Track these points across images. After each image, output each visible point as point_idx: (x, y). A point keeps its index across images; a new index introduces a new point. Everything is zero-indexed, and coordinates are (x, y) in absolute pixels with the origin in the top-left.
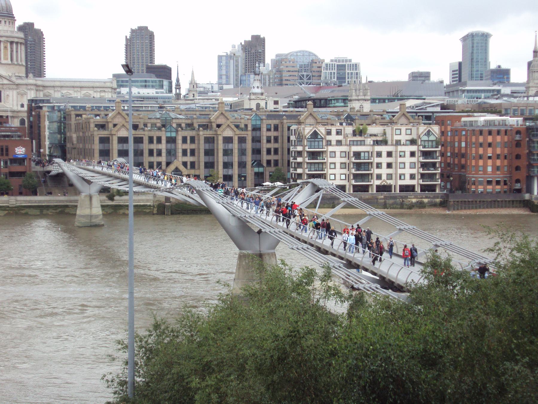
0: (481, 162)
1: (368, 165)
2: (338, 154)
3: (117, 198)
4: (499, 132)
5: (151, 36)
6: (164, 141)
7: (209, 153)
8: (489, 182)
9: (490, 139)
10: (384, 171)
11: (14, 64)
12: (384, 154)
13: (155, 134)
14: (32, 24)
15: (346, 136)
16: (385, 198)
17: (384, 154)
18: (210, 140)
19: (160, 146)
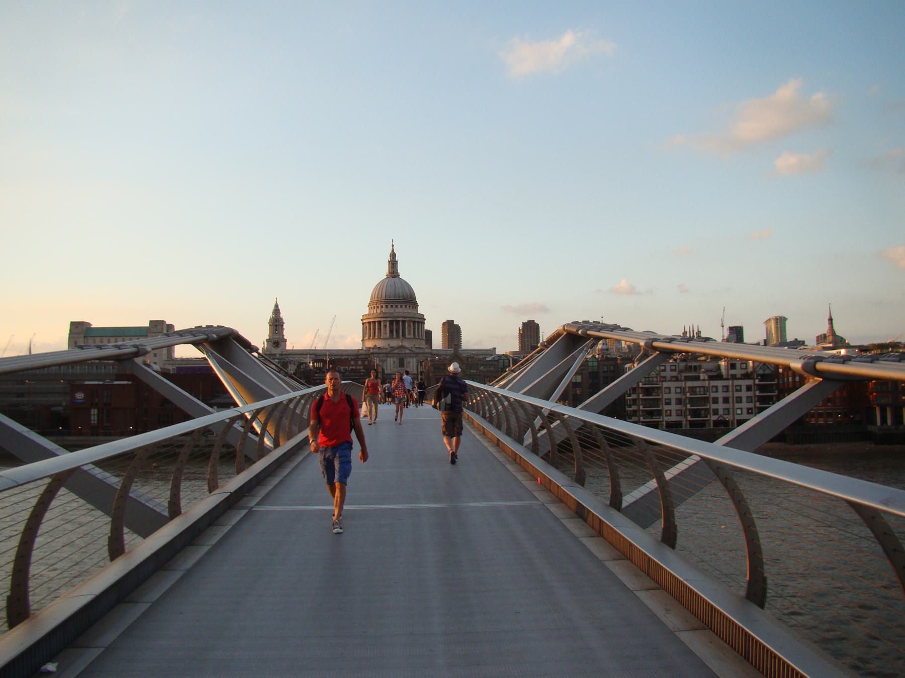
1: (705, 400)
2: (673, 390)
5: (537, 326)
10: (720, 406)
17: (720, 389)
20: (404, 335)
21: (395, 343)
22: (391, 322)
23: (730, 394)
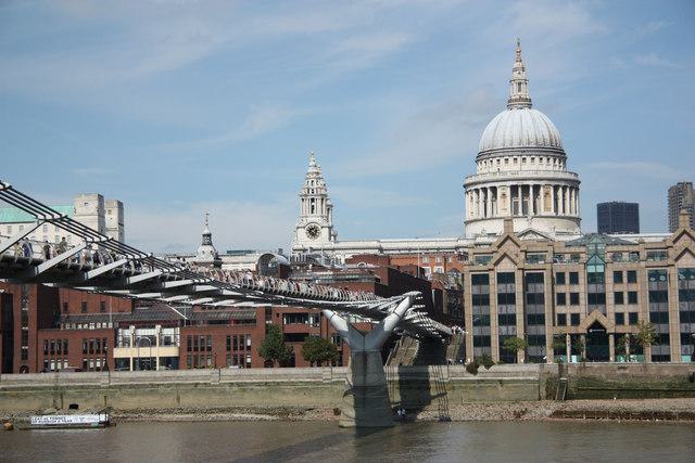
3: (482, 368)
6: (582, 279)
7: (658, 296)
11: (559, 217)
13: (566, 267)
19: (575, 289)
22: (514, 189)
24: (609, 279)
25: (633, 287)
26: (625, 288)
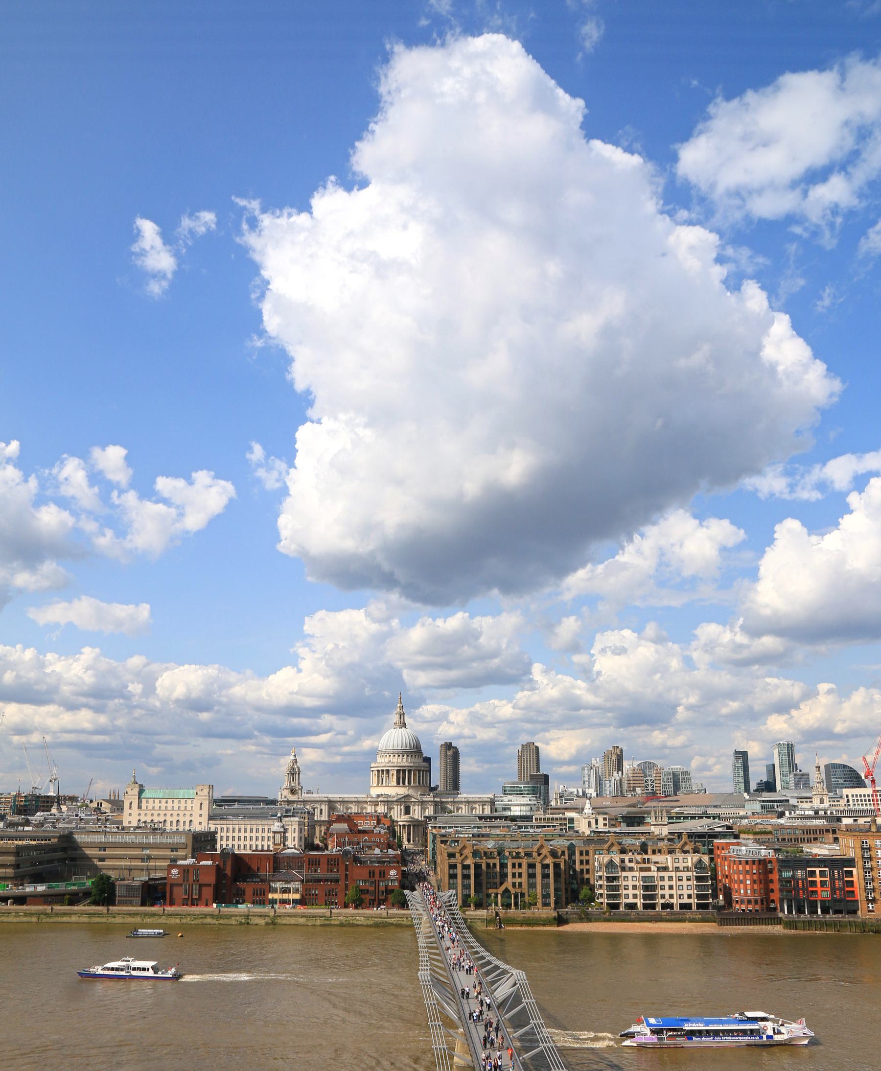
0: (742, 886)
1: (654, 888)
2: (630, 878)
4: (754, 862)
7: (532, 876)
8: (749, 902)
9: (747, 867)
10: (667, 892)
12: (666, 879)
14: (451, 744)
15: (637, 862)
16: (667, 914)
17: (666, 879)
18: (532, 866)
20: (409, 783)
21: (402, 791)
22: (398, 771)
23: (673, 883)
24: (510, 866)
25: (520, 870)
26: (517, 871)
